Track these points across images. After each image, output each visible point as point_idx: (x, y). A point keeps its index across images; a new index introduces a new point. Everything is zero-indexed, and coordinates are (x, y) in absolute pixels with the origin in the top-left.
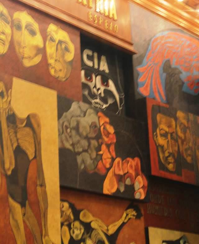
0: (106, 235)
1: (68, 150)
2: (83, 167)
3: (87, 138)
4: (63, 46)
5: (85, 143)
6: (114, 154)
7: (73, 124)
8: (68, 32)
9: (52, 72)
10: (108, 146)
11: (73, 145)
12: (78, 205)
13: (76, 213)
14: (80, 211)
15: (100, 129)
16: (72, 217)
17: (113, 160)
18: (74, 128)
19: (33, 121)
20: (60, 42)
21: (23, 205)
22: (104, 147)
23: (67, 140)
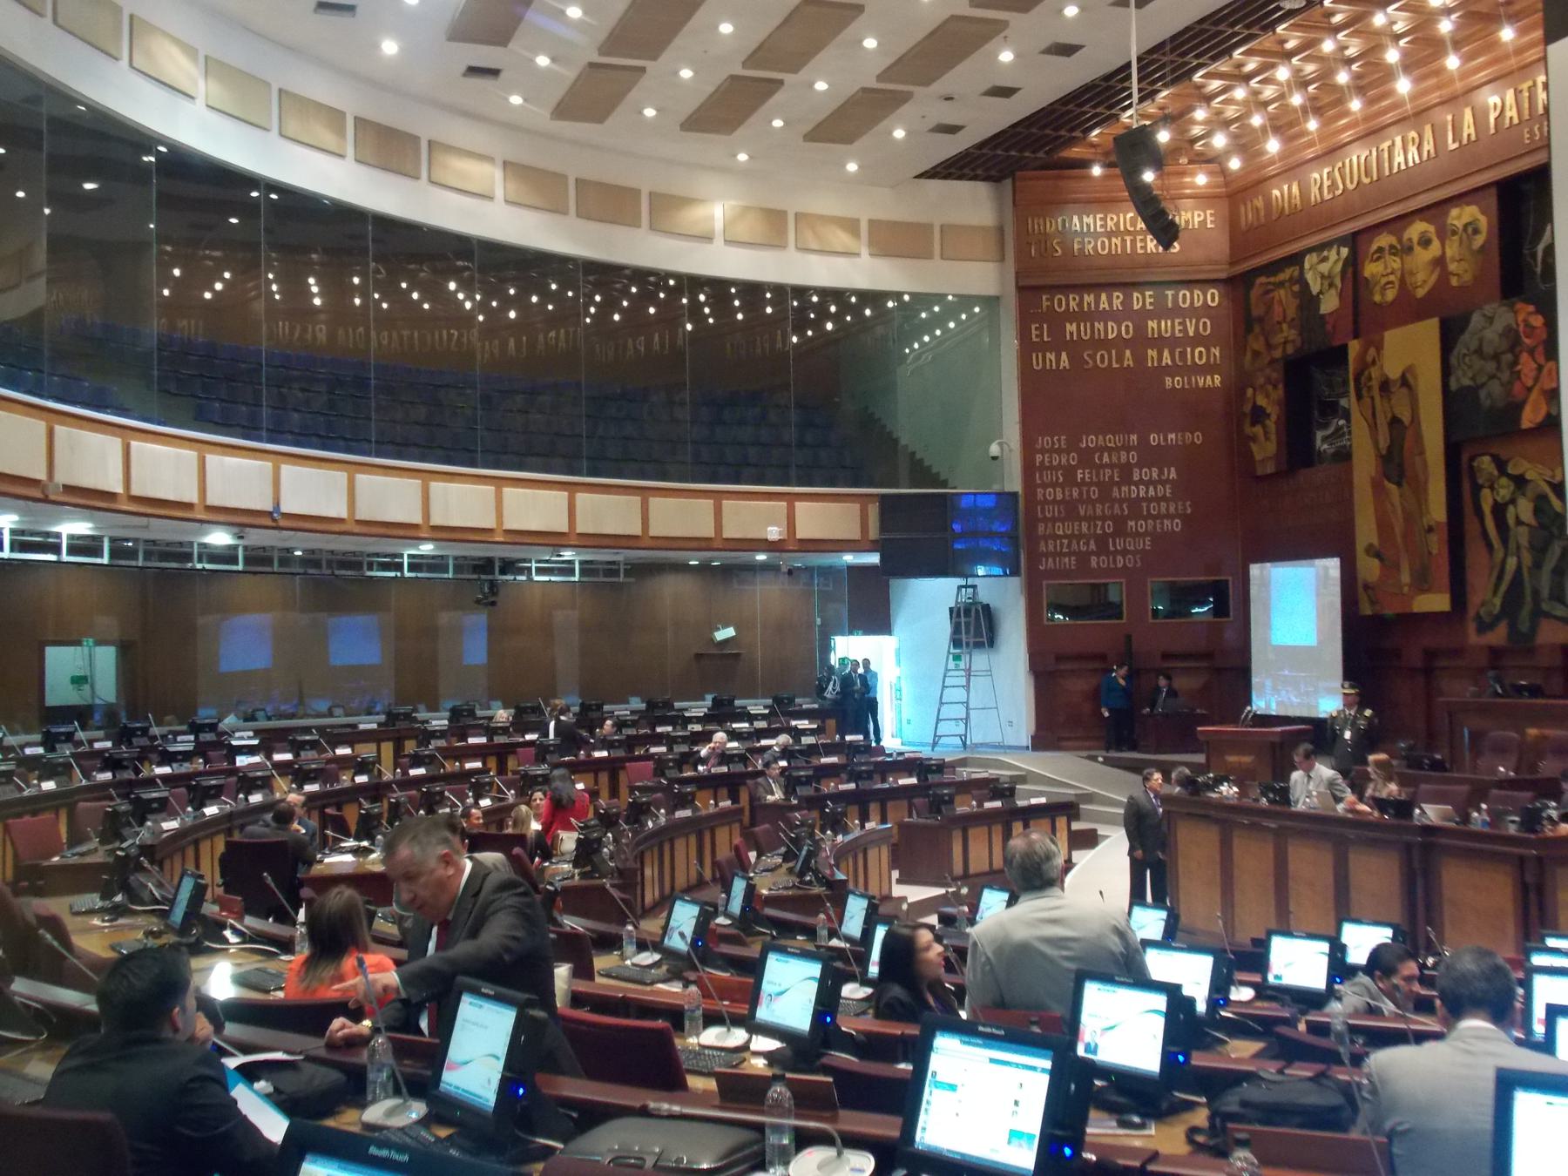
0: (1549, 483)
1: (1469, 387)
2: (1488, 402)
3: (1496, 357)
4: (1470, 230)
5: (1490, 366)
6: (1541, 360)
7: (1474, 345)
8: (1476, 203)
9: (1454, 282)
10: (1531, 352)
11: (1473, 379)
12: (1504, 456)
13: (1501, 465)
14: (1507, 462)
15: (1517, 332)
16: (1496, 473)
17: (1540, 368)
18: (1476, 352)
19: (1409, 376)
20: (1466, 226)
21: (1399, 484)
22: (1525, 357)
23: (1465, 374)
